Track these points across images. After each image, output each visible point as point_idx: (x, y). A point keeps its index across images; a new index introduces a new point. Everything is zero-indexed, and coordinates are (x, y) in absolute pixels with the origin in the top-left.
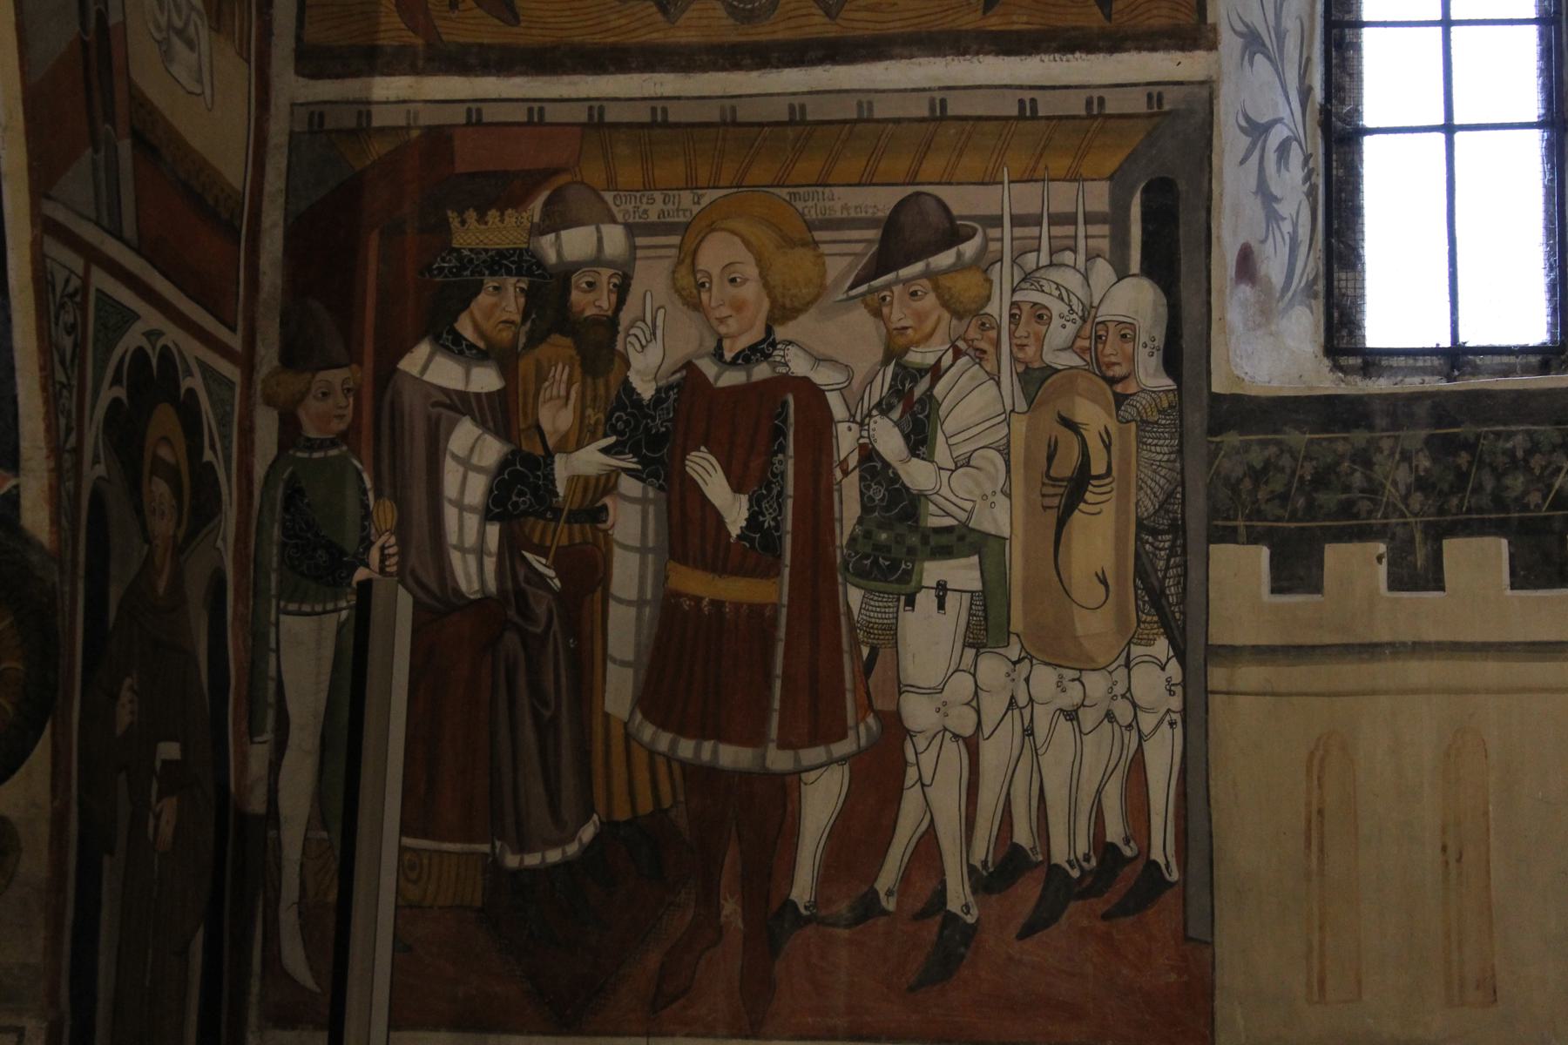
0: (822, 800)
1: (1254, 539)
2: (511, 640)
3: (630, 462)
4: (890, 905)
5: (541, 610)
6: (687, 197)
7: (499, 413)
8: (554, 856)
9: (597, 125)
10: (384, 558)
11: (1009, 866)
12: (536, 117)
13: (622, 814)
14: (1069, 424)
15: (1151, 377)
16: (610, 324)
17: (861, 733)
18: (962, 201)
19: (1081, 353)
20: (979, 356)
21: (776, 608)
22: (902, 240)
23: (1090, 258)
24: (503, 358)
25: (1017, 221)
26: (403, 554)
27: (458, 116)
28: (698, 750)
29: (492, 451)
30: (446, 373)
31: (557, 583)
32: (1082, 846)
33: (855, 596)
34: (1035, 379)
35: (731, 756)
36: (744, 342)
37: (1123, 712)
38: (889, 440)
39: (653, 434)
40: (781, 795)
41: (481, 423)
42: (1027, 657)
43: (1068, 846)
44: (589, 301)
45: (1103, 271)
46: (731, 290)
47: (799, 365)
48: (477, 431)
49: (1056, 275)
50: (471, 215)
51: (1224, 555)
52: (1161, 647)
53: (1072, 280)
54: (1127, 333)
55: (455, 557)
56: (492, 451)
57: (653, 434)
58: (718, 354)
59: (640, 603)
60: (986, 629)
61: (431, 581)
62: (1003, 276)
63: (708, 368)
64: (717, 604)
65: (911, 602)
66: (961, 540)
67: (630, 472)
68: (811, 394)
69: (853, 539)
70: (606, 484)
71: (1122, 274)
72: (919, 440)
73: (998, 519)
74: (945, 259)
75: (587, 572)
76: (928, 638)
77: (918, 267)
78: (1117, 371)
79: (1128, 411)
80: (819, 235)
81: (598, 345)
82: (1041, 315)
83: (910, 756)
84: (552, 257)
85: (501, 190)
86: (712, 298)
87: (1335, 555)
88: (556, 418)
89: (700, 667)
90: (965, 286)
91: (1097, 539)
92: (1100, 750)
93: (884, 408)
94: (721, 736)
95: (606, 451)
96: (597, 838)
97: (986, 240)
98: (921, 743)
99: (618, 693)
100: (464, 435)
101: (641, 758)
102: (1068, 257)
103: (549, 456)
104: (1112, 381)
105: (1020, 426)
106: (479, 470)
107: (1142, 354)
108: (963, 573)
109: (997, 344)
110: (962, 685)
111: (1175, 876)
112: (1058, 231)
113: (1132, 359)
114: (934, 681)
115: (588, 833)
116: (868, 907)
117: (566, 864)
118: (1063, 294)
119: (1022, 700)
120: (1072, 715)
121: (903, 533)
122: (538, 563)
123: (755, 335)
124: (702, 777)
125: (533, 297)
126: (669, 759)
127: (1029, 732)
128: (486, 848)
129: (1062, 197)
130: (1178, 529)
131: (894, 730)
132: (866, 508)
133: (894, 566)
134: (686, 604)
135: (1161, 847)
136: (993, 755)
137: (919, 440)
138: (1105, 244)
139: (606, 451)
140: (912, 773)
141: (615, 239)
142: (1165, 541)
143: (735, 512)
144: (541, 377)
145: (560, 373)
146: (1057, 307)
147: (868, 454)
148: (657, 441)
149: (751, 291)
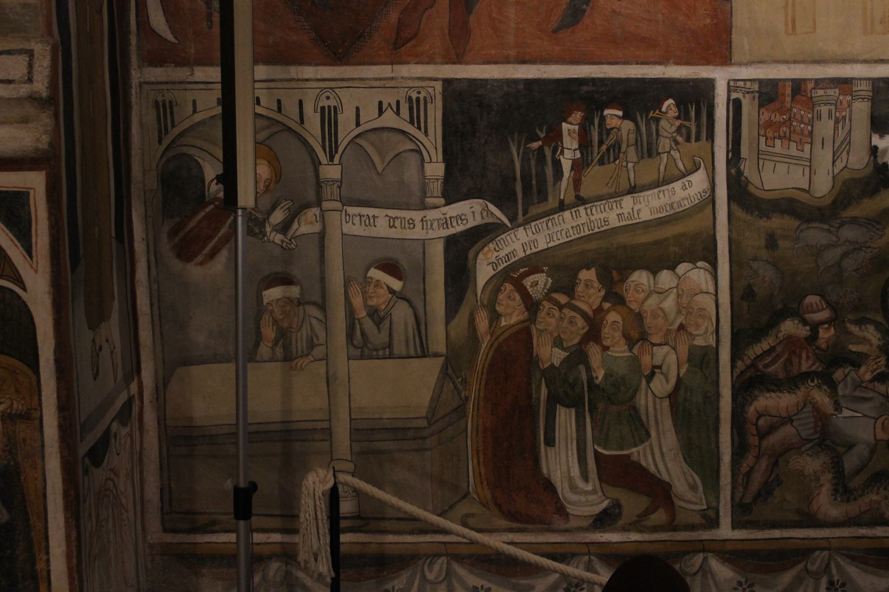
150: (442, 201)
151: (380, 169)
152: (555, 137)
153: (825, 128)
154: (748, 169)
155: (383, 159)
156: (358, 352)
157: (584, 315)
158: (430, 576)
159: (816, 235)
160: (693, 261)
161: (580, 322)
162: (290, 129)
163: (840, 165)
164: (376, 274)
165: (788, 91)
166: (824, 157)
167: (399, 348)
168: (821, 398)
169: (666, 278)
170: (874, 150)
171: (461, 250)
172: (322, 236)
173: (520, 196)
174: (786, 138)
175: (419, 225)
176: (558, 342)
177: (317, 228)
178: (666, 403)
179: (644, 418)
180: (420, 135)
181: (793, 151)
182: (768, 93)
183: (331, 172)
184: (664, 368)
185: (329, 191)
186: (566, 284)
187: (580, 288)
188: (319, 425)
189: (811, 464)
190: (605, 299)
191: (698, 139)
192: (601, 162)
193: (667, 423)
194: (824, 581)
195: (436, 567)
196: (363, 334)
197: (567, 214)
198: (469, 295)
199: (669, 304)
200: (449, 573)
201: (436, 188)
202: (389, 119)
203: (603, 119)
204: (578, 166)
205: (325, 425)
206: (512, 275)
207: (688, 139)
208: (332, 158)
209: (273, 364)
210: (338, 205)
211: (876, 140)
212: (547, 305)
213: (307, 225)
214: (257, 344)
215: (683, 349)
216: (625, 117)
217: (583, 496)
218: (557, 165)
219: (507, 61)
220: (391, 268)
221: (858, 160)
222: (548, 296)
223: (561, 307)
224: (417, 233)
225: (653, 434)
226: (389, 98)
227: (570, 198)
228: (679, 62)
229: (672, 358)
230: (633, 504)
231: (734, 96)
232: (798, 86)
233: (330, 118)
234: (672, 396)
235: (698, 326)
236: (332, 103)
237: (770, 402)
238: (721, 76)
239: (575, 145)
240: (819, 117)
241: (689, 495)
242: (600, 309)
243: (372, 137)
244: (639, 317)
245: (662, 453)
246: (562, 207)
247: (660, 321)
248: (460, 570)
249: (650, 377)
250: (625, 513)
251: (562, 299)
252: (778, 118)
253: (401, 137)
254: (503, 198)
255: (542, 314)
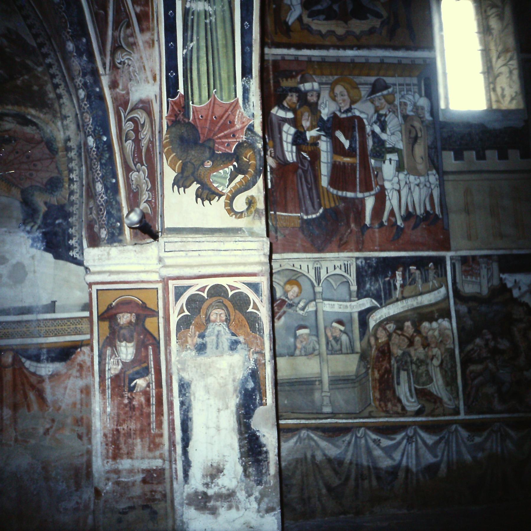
0: (370, 203)
1: (450, 150)
2: (300, 171)
3: (323, 133)
4: (386, 224)
5: (306, 164)
6: (331, 77)
7: (295, 122)
8: (314, 216)
9: (310, 61)
10: (271, 153)
11: (408, 216)
12: (296, 59)
13: (328, 207)
14: (413, 126)
15: (428, 117)
16: (316, 104)
17: (376, 189)
18: (389, 80)
19: (414, 112)
20: (394, 112)
21: (356, 164)
22: (376, 88)
23: (415, 92)
24: (294, 111)
25: (400, 85)
26: (275, 152)
27: (279, 58)
28: (342, 194)
29: (293, 130)
30: (281, 114)
31: (309, 159)
32: (422, 211)
33: (373, 161)
34: (405, 117)
35: (350, 195)
36: (345, 108)
37: (428, 185)
38: (377, 129)
39: (329, 127)
40: (362, 201)
41: (289, 124)
42: (408, 173)
43: (419, 211)
44: (312, 99)
45: (417, 96)
46: (342, 97)
47: (357, 113)
48: (289, 126)
49: (408, 96)
50: (284, 79)
51: (444, 153)
52: (434, 172)
53: (411, 97)
54: (423, 108)
55: (286, 153)
56: (293, 130)
57: (329, 127)
58: (340, 111)
59: (327, 163)
60: (400, 168)
61: (281, 157)
62: (397, 96)
63: (338, 113)
64: (344, 163)
65: (384, 162)
66: (393, 150)
67: (323, 135)
68: (360, 120)
69: (372, 150)
70: (319, 137)
71: (421, 96)
72: (383, 129)
73: (400, 145)
74: (385, 92)
75: (315, 155)
76: (388, 169)
77: (380, 94)
78: (422, 116)
79: (424, 124)
80: (359, 86)
81: (314, 108)
82: (405, 104)
83: (387, 194)
84: (303, 89)
85: (289, 75)
86: (339, 98)
87: (466, 154)
88: (306, 124)
89: (341, 176)
90: (390, 98)
91: (420, 150)
92: (424, 191)
93: (375, 122)
94: (347, 190)
95: (318, 131)
96: (323, 212)
97: (394, 89)
98: (389, 191)
99: (324, 182)
100: (286, 127)
101: (331, 196)
102: (410, 93)
103: (305, 132)
104: (421, 118)
105: (403, 126)
106: (290, 134)
107: (426, 113)
108: (394, 157)
109: (397, 110)
110: (396, 179)
111: (441, 216)
112: (408, 87)
113: (424, 114)
114: (390, 178)
115: (321, 211)
116: (381, 225)
117: (317, 218)
118: (410, 100)
119: (408, 182)
120: (418, 185)
121: (381, 150)
122: (305, 154)
123: (347, 107)
124: (344, 199)
125: (299, 99)
126: (337, 195)
127: (410, 189)
128: (299, 215)
129: (408, 80)
130: (436, 148)
131: (383, 189)
132: (374, 143)
133: (380, 155)
134: (337, 163)
135: (438, 211)
136: (404, 192)
137: (383, 129)
138: (417, 90)
139: (318, 131)
140: (387, 198)
141: (316, 86)
142: (434, 150)
143: (347, 144)
144: (302, 115)
145: (306, 114)
146: (409, 103)
147: (373, 132)
148: (329, 129)
149: (346, 97)
150: (357, 299)
151: (335, 287)
152: (394, 276)
153: (484, 272)
154: (459, 286)
155: (336, 285)
156: (330, 352)
157: (407, 337)
158: (359, 435)
159: (484, 309)
160: (443, 318)
161: (406, 340)
162: (304, 275)
163: (490, 284)
164: (335, 324)
165: (471, 259)
166: (484, 282)
167: (344, 350)
168: (491, 365)
169: (435, 325)
170: (501, 279)
171: (364, 316)
172: (316, 312)
173: (383, 297)
174: (472, 275)
175: (349, 307)
176: (399, 347)
177: (314, 309)
178: (438, 369)
179: (431, 374)
180: (348, 276)
181: (474, 279)
182: (464, 260)
183: (318, 289)
184: (437, 356)
185: (318, 296)
186: (400, 327)
187: (405, 328)
188: (317, 379)
189: (490, 390)
190: (414, 332)
191: (442, 276)
192: (410, 284)
193: (439, 376)
194: (499, 434)
195: (360, 432)
196: (332, 346)
197: (399, 303)
198: (367, 332)
199: (436, 333)
200: (365, 435)
201: (354, 294)
202: (338, 271)
203: (409, 270)
204: (402, 286)
205: (320, 379)
206: (381, 324)
207: (438, 276)
208: (319, 284)
209: (300, 357)
210: (321, 301)
211: (501, 276)
212: (394, 335)
213: (311, 308)
214: (295, 349)
215: (443, 349)
216: (417, 269)
217: (411, 404)
218: (395, 286)
219: (376, 251)
220: (340, 322)
221: (496, 282)
222: (395, 332)
223: (399, 335)
224: (348, 310)
225: (434, 380)
226: (338, 264)
227: (400, 297)
228: (434, 250)
229: (439, 352)
230: (429, 407)
231: (453, 261)
232: (474, 257)
233: (317, 271)
234: (441, 365)
235: (447, 341)
236: (318, 266)
237: (473, 368)
238: (448, 255)
239: (401, 279)
240: (482, 267)
241: (449, 403)
242: (413, 335)
243: (332, 277)
244: (426, 338)
245: (438, 386)
246: (397, 300)
247: (434, 339)
248: (370, 433)
249: (432, 359)
250: (426, 409)
251: (399, 332)
252: (468, 269)
253: (342, 277)
254: (377, 297)
255: (393, 338)
